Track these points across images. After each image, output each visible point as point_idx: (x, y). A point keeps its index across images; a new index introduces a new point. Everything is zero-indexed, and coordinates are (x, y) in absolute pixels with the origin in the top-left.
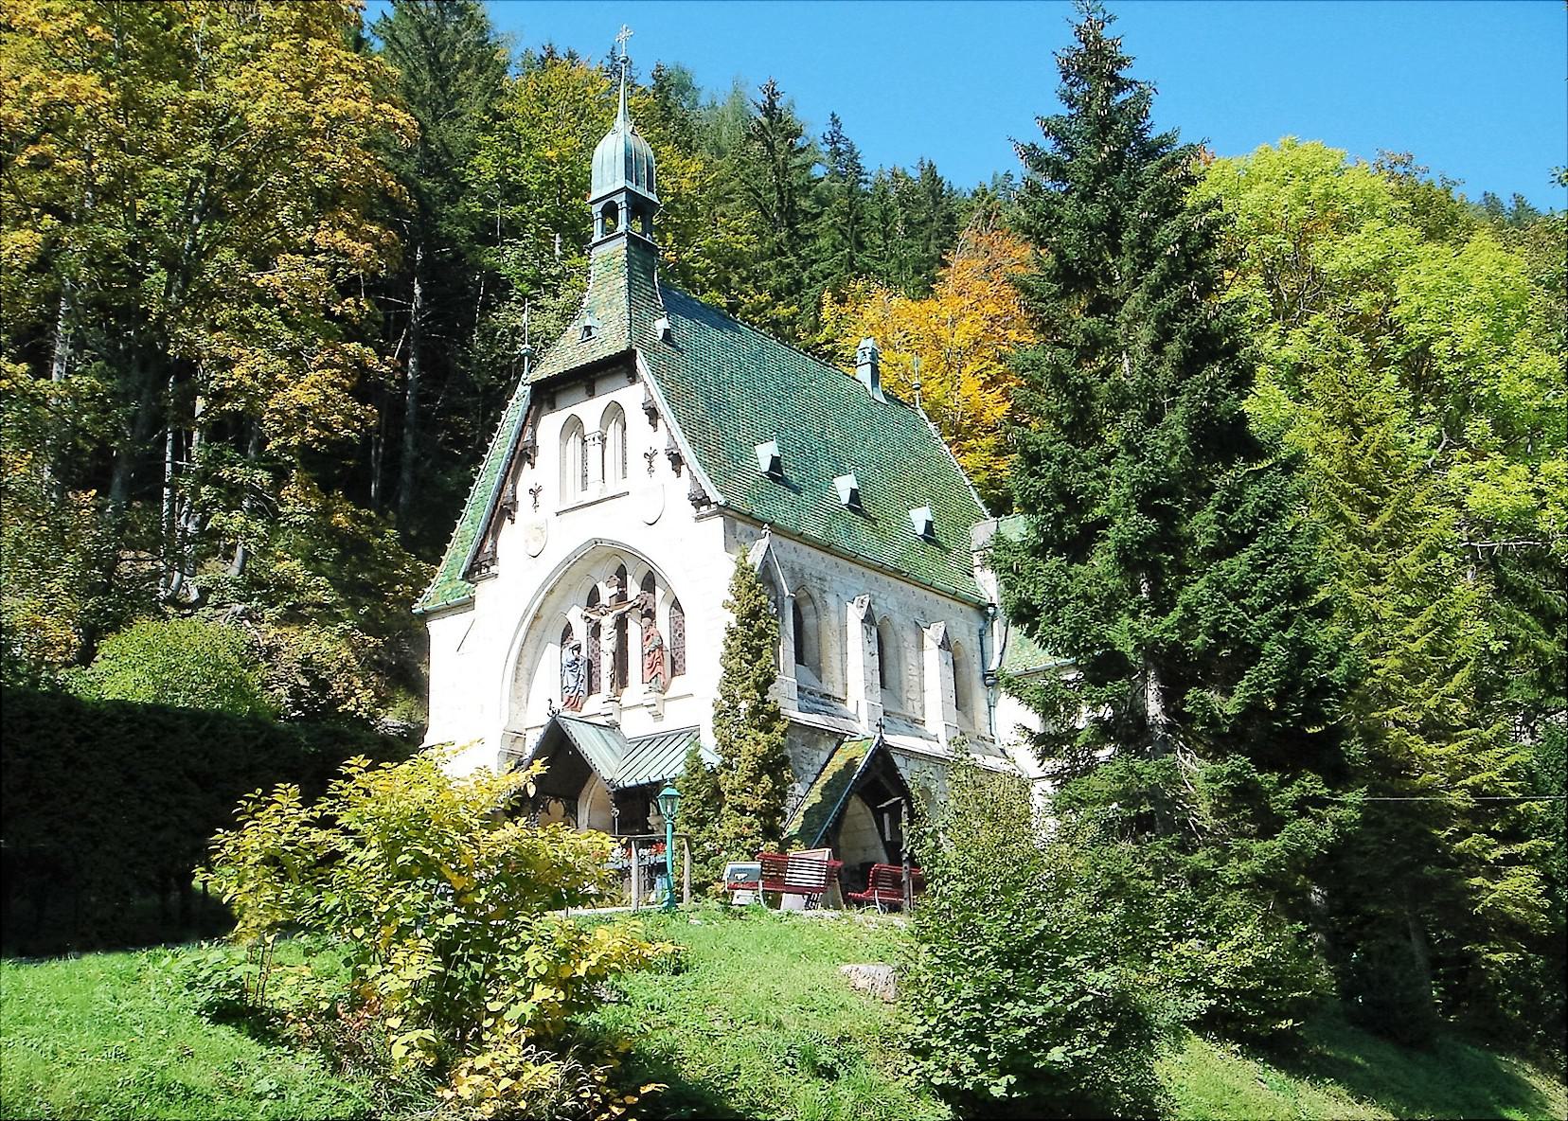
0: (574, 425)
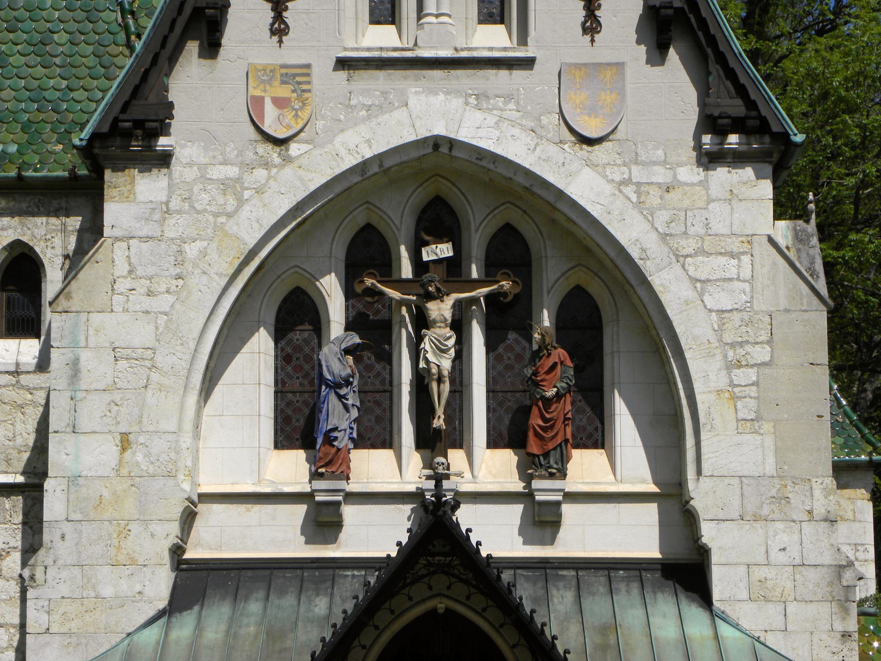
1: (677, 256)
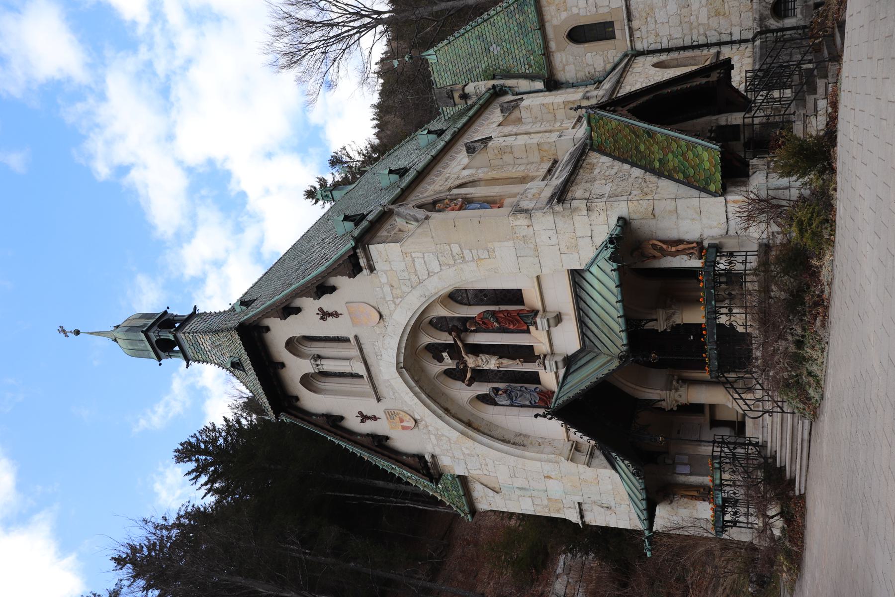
0: (307, 381)
1: (420, 283)
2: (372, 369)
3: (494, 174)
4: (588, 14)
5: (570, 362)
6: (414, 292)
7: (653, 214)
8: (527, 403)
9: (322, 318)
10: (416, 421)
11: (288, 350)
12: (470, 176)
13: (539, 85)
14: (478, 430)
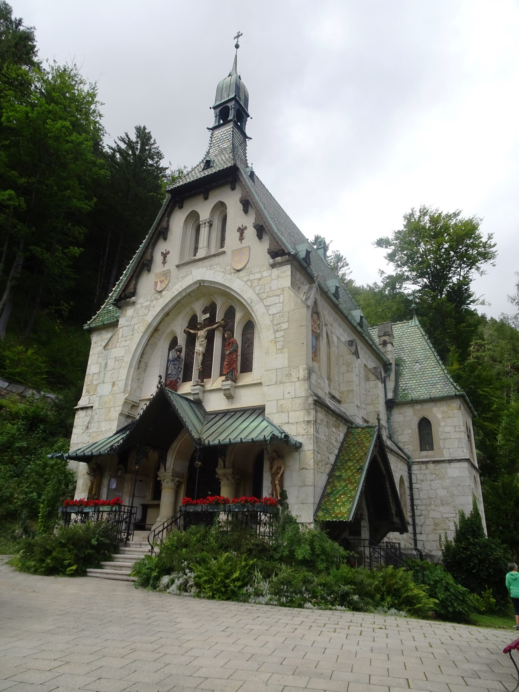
0: (194, 216)
1: (261, 299)
2: (200, 263)
3: (333, 358)
4: (440, 433)
5: (198, 404)
6: (255, 295)
7: (303, 468)
8: (169, 372)
9: (239, 228)
10: (161, 292)
11: (217, 203)
12: (333, 341)
13: (390, 396)
14: (151, 336)
